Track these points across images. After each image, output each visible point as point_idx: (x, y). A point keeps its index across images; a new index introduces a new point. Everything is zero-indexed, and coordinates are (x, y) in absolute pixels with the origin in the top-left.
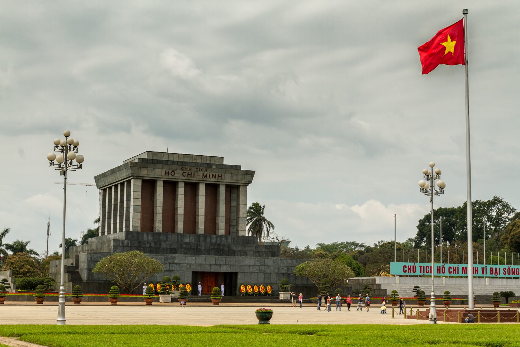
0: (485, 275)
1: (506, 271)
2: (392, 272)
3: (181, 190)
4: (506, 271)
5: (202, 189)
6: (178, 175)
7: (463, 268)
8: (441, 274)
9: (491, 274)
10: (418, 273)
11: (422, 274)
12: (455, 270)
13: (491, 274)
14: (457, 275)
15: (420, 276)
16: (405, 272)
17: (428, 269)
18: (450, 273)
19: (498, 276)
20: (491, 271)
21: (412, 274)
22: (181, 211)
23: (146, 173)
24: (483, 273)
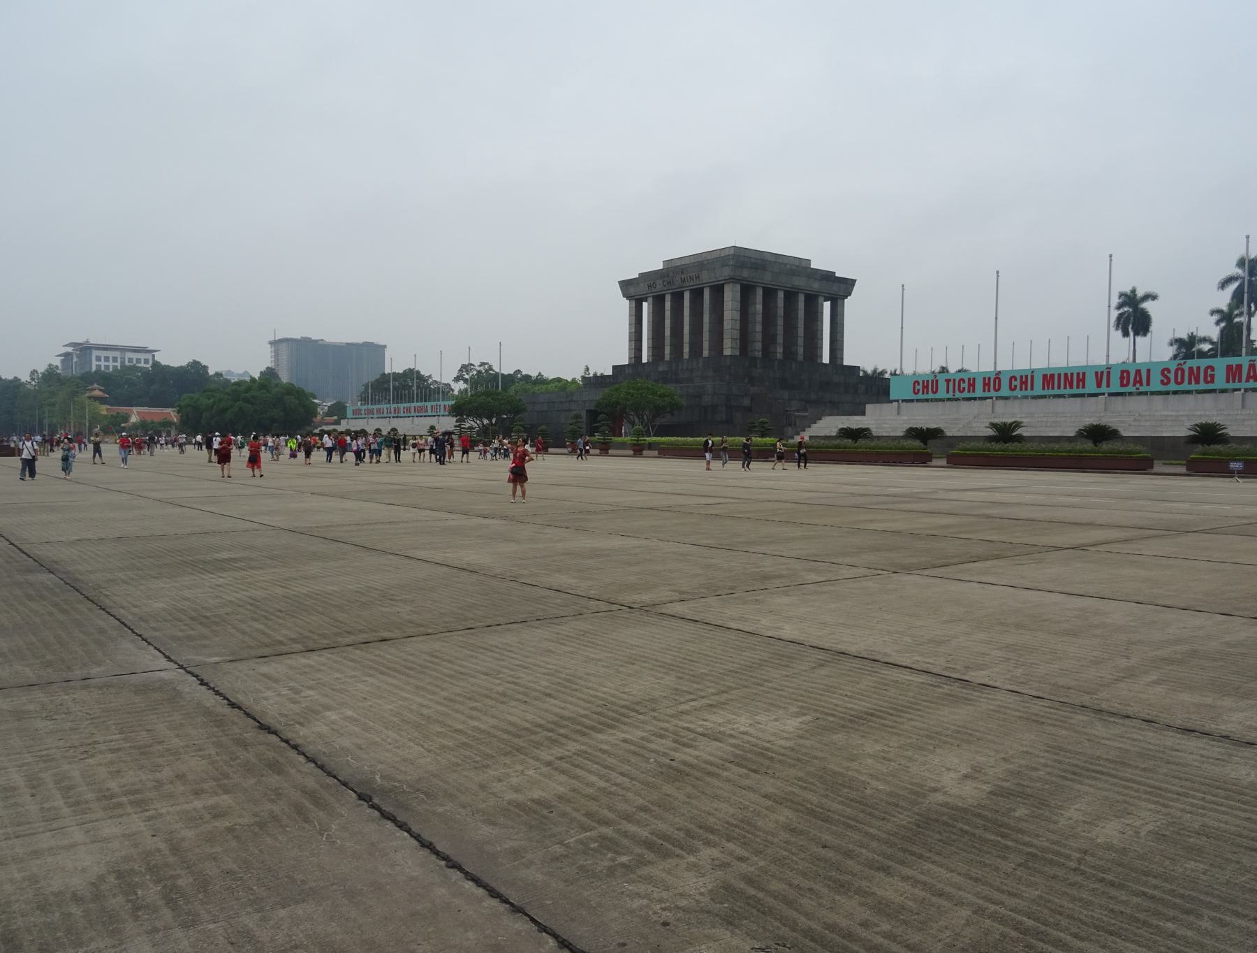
0: (1104, 389)
1: (1172, 376)
2: (892, 398)
3: (668, 305)
4: (1172, 376)
5: (687, 296)
6: (659, 286)
7: (1229, 368)
8: (992, 393)
9: (1122, 385)
10: (942, 393)
11: (950, 395)
12: (1026, 382)
13: (1122, 385)
14: (1029, 392)
15: (949, 399)
16: (916, 393)
17: (962, 385)
18: (1012, 389)
19: (1144, 388)
20: (1122, 378)
21: (931, 396)
22: (667, 332)
23: (632, 291)
24: (1099, 385)
